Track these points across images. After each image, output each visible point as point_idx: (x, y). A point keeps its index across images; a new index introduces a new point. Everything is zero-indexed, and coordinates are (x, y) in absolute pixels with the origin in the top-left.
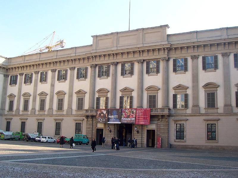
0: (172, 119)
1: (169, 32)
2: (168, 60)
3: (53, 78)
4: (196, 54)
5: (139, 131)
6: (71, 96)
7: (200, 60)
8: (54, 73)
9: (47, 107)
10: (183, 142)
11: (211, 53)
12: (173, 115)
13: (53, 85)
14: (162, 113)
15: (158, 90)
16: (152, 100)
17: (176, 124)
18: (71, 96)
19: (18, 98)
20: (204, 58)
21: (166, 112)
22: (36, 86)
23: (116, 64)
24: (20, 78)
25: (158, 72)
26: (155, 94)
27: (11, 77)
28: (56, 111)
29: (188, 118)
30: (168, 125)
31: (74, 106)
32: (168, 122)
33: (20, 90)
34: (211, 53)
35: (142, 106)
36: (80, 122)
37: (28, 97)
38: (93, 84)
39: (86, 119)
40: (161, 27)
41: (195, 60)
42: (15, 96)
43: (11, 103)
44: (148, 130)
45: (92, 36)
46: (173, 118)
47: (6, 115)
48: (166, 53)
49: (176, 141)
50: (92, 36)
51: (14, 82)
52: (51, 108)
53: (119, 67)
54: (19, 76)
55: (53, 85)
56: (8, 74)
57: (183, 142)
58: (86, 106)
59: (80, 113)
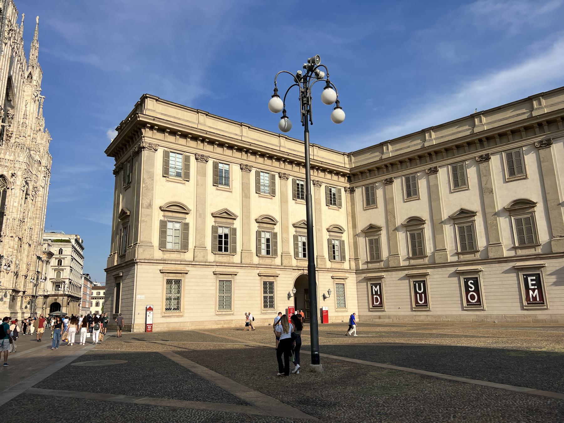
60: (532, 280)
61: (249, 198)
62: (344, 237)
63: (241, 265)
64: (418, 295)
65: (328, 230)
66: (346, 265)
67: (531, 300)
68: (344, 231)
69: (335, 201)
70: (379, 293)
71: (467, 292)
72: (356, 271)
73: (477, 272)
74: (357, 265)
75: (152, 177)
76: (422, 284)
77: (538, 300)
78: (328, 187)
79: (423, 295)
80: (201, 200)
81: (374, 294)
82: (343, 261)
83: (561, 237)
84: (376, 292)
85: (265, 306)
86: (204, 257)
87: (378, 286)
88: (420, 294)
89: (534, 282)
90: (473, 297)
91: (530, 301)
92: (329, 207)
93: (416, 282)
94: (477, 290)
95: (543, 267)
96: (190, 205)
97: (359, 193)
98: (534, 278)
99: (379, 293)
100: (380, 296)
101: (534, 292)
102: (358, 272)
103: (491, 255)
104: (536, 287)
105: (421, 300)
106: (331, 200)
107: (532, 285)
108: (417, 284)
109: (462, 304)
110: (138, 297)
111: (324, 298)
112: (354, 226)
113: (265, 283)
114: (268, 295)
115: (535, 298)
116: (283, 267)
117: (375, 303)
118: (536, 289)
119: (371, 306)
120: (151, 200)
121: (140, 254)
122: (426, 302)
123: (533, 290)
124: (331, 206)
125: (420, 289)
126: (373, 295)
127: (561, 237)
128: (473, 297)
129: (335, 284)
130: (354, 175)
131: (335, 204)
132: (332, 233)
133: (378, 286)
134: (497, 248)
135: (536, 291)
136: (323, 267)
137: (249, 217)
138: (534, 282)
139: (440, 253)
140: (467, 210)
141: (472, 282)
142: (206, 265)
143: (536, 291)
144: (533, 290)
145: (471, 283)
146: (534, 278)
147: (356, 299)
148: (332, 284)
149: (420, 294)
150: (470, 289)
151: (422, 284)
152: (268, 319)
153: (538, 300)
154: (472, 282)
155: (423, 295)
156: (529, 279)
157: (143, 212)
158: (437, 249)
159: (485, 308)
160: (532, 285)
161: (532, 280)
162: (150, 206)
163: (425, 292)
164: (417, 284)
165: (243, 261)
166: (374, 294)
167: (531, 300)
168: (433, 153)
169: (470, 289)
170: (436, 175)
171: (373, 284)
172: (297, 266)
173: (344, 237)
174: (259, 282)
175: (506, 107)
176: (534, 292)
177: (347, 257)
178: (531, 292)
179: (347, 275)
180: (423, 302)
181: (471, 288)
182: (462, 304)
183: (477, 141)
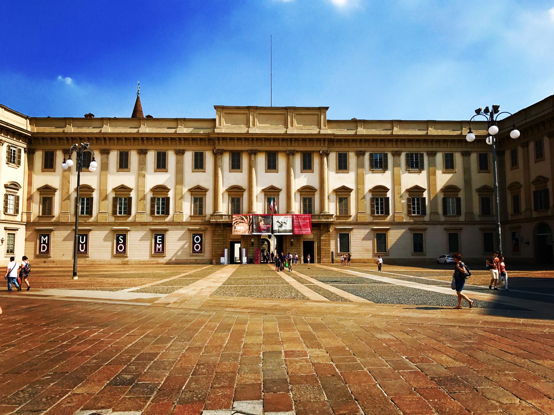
1: (330, 115)
4: (363, 149)
7: (367, 156)
8: (143, 156)
11: (381, 149)
17: (340, 234)
20: (371, 155)
34: (381, 149)
36: (201, 233)
41: (361, 157)
42: (55, 190)
44: (304, 242)
45: (216, 107)
48: (326, 145)
50: (216, 107)
58: (209, 210)
60: (159, 238)
62: (20, 193)
64: (80, 245)
65: (6, 187)
66: (18, 218)
67: (157, 250)
68: (21, 187)
69: (14, 159)
70: (47, 243)
71: (118, 244)
72: (26, 223)
73: (127, 231)
74: (29, 217)
76: (85, 237)
77: (161, 250)
78: (9, 146)
79: (84, 245)
81: (42, 243)
82: (16, 214)
83: (180, 212)
84: (44, 242)
87: (47, 238)
88: (82, 245)
89: (161, 239)
90: (121, 248)
91: (156, 251)
92: (9, 165)
93: (80, 235)
94: (124, 243)
97: (39, 157)
98: (161, 237)
99: (47, 243)
100: (48, 245)
101: (159, 246)
102: (28, 225)
103: (138, 220)
104: (161, 242)
105: (82, 249)
106: (11, 159)
107: (159, 241)
108: (81, 237)
109: (113, 252)
112: (30, 184)
115: (159, 249)
117: (42, 251)
118: (160, 244)
119: (38, 253)
122: (86, 250)
123: (159, 244)
124: (10, 164)
125: (83, 241)
126: (40, 244)
127: (180, 212)
128: (121, 248)
129: (7, 234)
130: (35, 138)
131: (14, 162)
132: (8, 189)
133: (47, 238)
134: (142, 215)
135: (161, 245)
138: (161, 239)
139: (102, 215)
140: (127, 187)
141: (122, 237)
143: (161, 245)
144: (159, 244)
145: (121, 238)
146: (161, 237)
147: (24, 246)
148: (5, 233)
149: (82, 245)
150: (120, 242)
151: (85, 237)
153: (161, 250)
154: (122, 237)
155: (84, 245)
156: (158, 237)
158: (100, 212)
159: (128, 255)
160: (159, 241)
161: (159, 238)
163: (86, 243)
164: (81, 237)
166: (42, 243)
167: (157, 250)
168: (107, 139)
169: (120, 242)
170: (107, 156)
171: (42, 235)
173: (20, 193)
175: (162, 120)
176: (159, 246)
177: (20, 211)
178: (157, 245)
180: (83, 250)
181: (121, 241)
182: (113, 252)
183: (140, 139)
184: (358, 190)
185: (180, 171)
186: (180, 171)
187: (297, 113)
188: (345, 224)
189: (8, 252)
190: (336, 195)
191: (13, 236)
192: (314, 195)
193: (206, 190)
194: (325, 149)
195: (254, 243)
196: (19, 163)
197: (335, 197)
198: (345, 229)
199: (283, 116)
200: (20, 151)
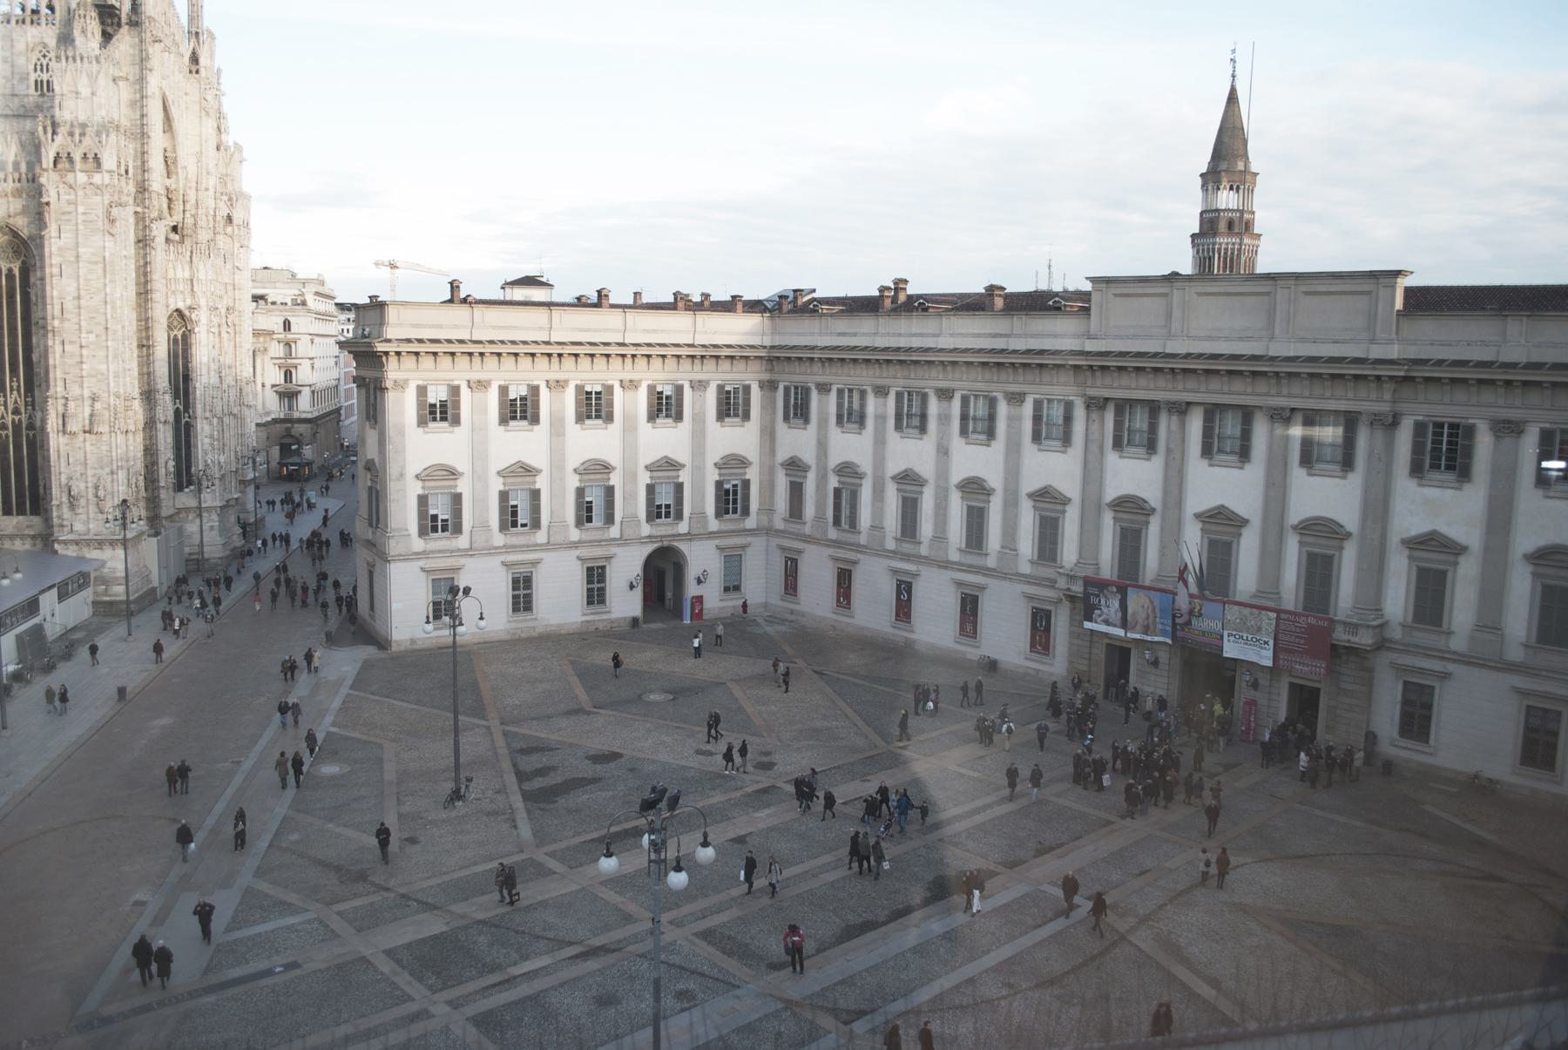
0: (1383, 661)
2: (1394, 423)
3: (944, 419)
5: (1261, 682)
6: (1011, 503)
9: (926, 528)
10: (1423, 753)
12: (1393, 646)
13: (943, 451)
14: (1346, 637)
15: (1343, 539)
16: (1319, 572)
18: (1011, 503)
19: (817, 476)
21: (1365, 639)
22: (880, 442)
23: (1182, 409)
24: (820, 401)
25: (1347, 462)
26: (1332, 552)
27: (787, 389)
28: (960, 550)
29: (1451, 667)
30: (1370, 684)
31: (1027, 545)
32: (1371, 670)
33: (822, 447)
35: (1277, 587)
37: (857, 481)
38: (1092, 474)
39: (1066, 603)
40: (1373, 275)
41: (1508, 442)
43: (796, 490)
46: (1393, 656)
47: (779, 533)
48: (1388, 396)
49: (1396, 743)
51: (798, 410)
52: (940, 537)
53: (1195, 424)
54: (814, 395)
55: (943, 451)
56: (776, 377)
57: (1423, 753)
58: (1069, 553)
59: (1046, 572)
61: (564, 435)
63: (548, 546)
75: (402, 433)
80: (479, 453)
85: (590, 602)
86: (487, 541)
95: (984, 588)
96: (462, 465)
110: (394, 605)
111: (699, 581)
113: (590, 570)
114: (596, 586)
116: (622, 541)
120: (403, 467)
121: (394, 547)
131: (736, 415)
136: (702, 531)
137: (562, 468)
142: (491, 551)
152: (594, 621)
157: (393, 487)
162: (402, 475)
165: (552, 539)
172: (650, 537)
174: (579, 568)
179: (749, 539)
184: (1487, 549)
185: (1013, 450)
186: (1013, 450)
187: (1304, 289)
188: (1426, 652)
189: (727, 589)
190: (1410, 558)
191: (738, 558)
192: (1341, 548)
193: (1066, 501)
194: (1384, 408)
195: (1161, 660)
196: (746, 416)
197: (1405, 562)
198: (1422, 671)
199: (1266, 298)
200: (747, 389)
